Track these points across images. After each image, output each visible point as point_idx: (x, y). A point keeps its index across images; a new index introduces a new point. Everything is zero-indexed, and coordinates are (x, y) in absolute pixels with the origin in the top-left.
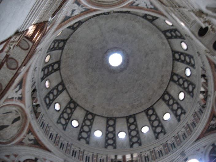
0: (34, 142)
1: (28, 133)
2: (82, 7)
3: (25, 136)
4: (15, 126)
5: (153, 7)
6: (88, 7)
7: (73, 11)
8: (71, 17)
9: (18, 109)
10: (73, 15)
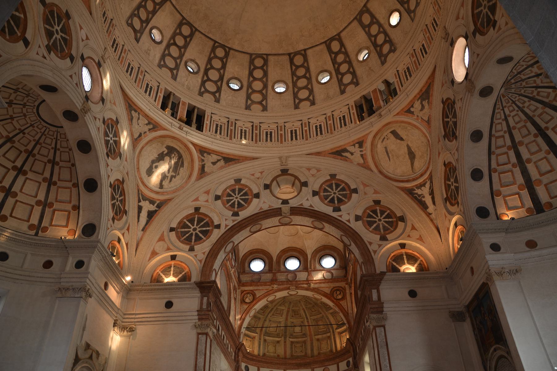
0: (424, 100)
1: (412, 113)
2: (203, 160)
3: (418, 116)
4: (407, 135)
5: (133, 112)
6: (198, 156)
7: (214, 163)
8: (222, 157)
9: (379, 138)
10: (220, 158)
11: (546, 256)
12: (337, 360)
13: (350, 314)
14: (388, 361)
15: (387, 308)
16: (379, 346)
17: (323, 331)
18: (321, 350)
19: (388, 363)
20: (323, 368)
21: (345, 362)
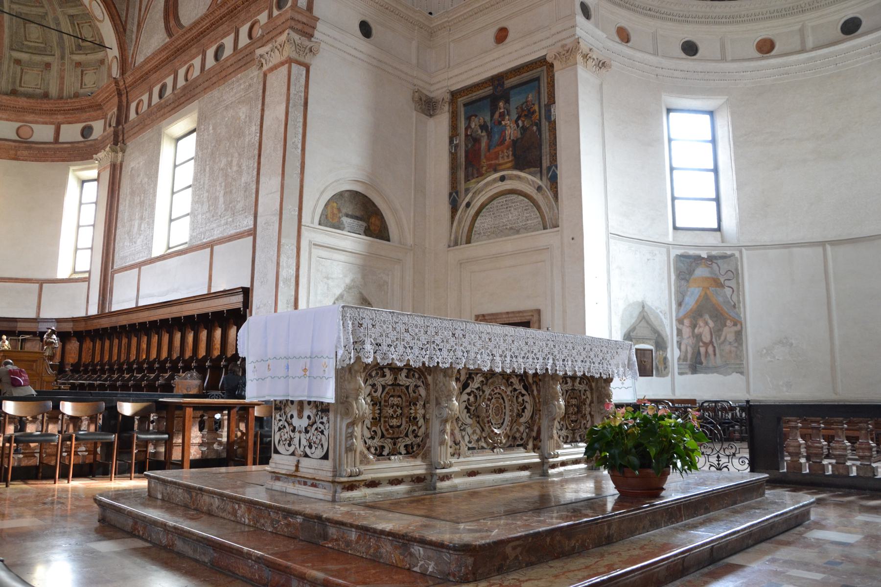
11: (637, 63)
12: (59, 117)
13: (128, 32)
14: (300, 137)
15: (322, 31)
16: (291, 102)
17: (36, 48)
18: (20, 86)
19: (300, 141)
20: (18, 124)
21: (81, 126)
